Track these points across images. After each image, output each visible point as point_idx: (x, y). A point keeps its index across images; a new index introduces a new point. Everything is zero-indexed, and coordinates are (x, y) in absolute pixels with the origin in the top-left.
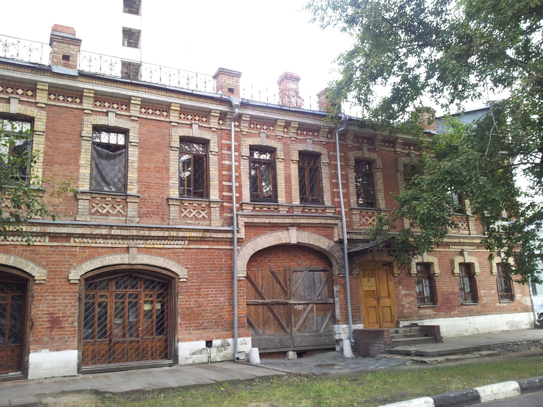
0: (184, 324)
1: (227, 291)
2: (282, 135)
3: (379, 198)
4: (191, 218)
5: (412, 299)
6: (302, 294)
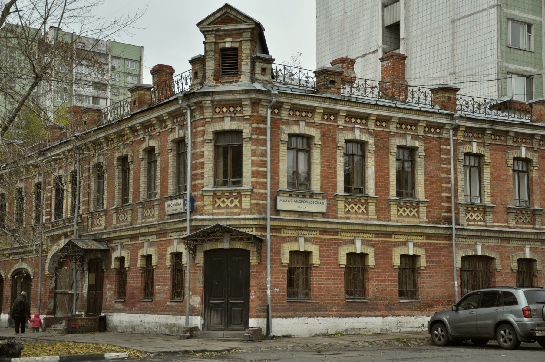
5: (112, 293)
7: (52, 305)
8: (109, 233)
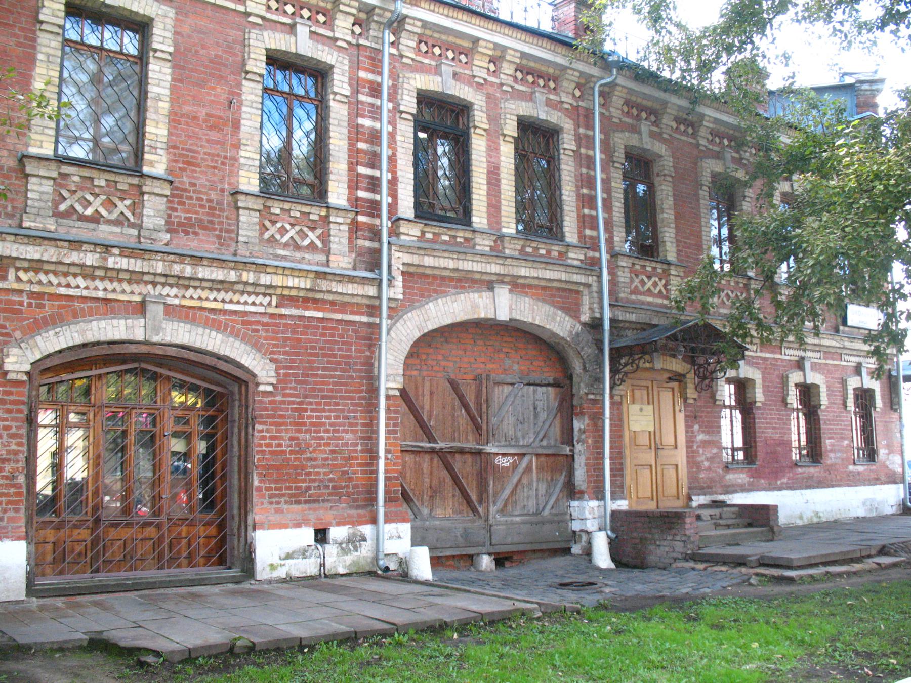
0: (267, 489)
1: (361, 419)
2: (486, 76)
3: (666, 239)
4: (286, 245)
6: (511, 432)
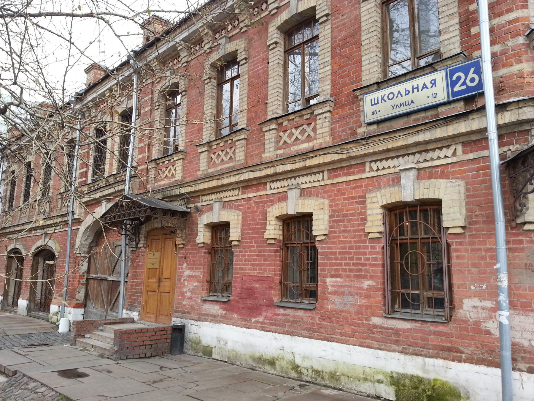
7: (81, 296)
8: (195, 181)
